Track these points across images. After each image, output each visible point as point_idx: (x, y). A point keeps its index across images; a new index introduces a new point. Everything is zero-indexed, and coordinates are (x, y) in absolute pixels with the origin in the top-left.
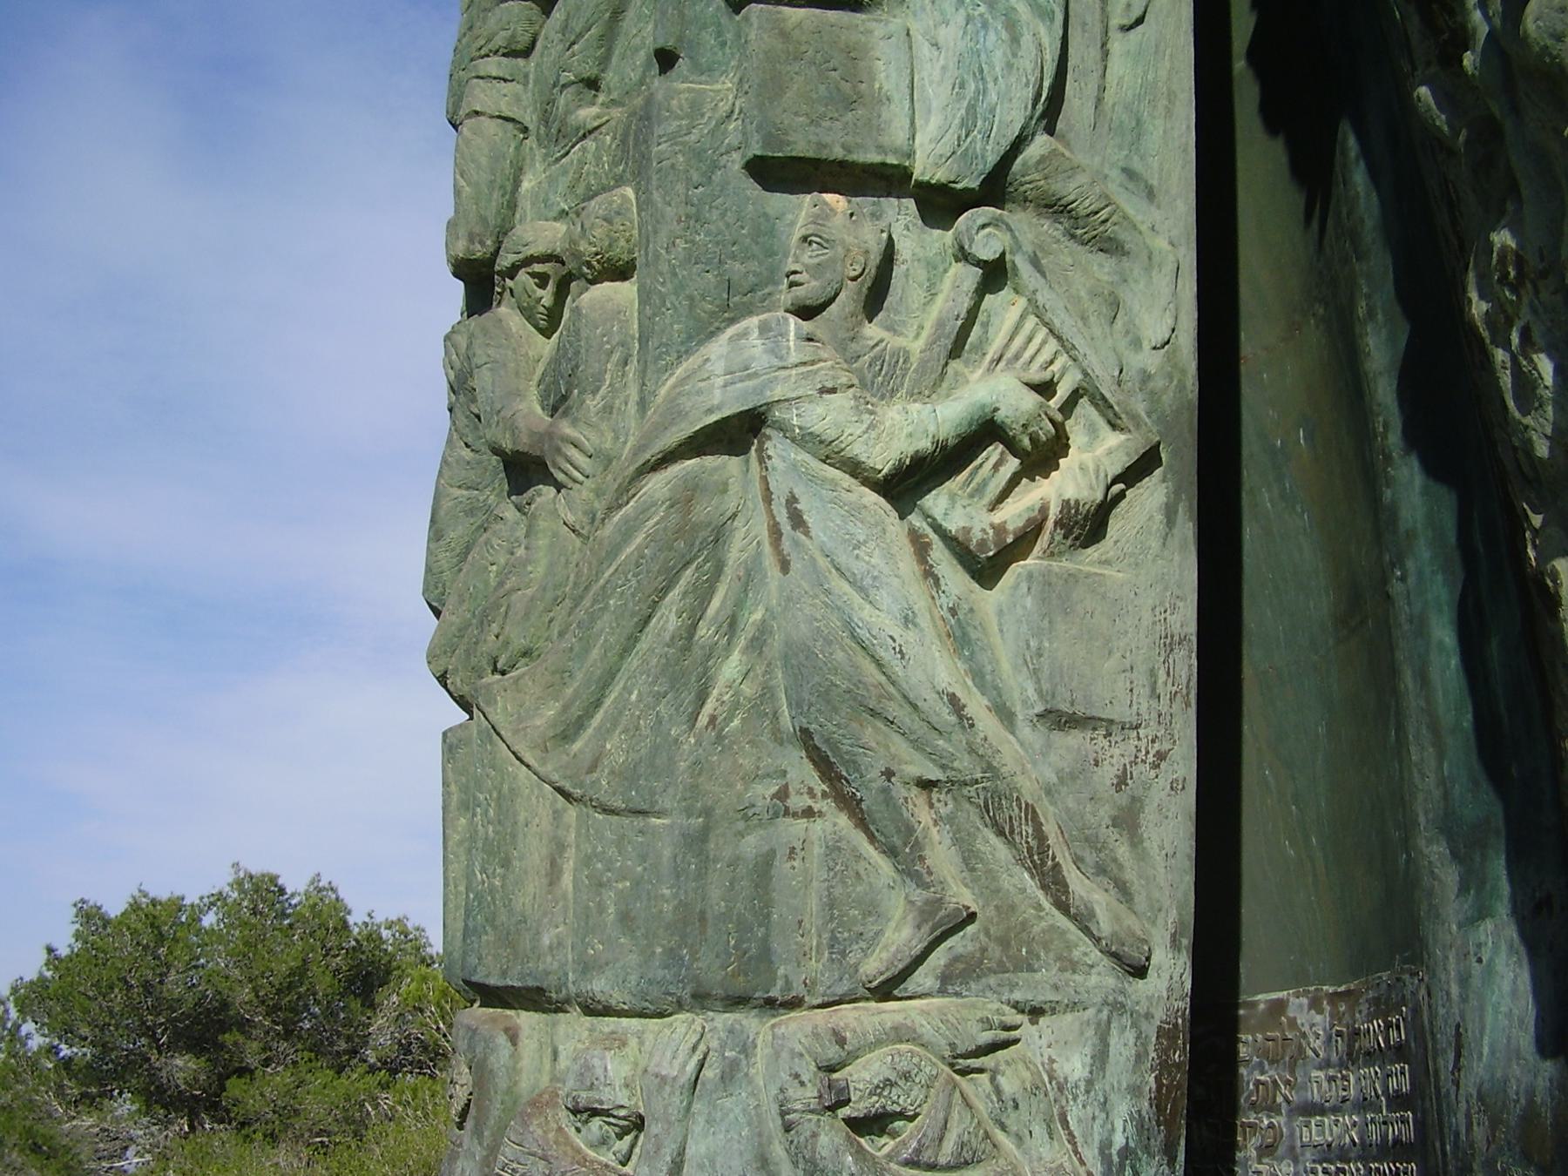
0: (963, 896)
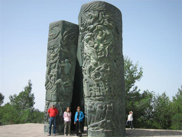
0: (65, 98)
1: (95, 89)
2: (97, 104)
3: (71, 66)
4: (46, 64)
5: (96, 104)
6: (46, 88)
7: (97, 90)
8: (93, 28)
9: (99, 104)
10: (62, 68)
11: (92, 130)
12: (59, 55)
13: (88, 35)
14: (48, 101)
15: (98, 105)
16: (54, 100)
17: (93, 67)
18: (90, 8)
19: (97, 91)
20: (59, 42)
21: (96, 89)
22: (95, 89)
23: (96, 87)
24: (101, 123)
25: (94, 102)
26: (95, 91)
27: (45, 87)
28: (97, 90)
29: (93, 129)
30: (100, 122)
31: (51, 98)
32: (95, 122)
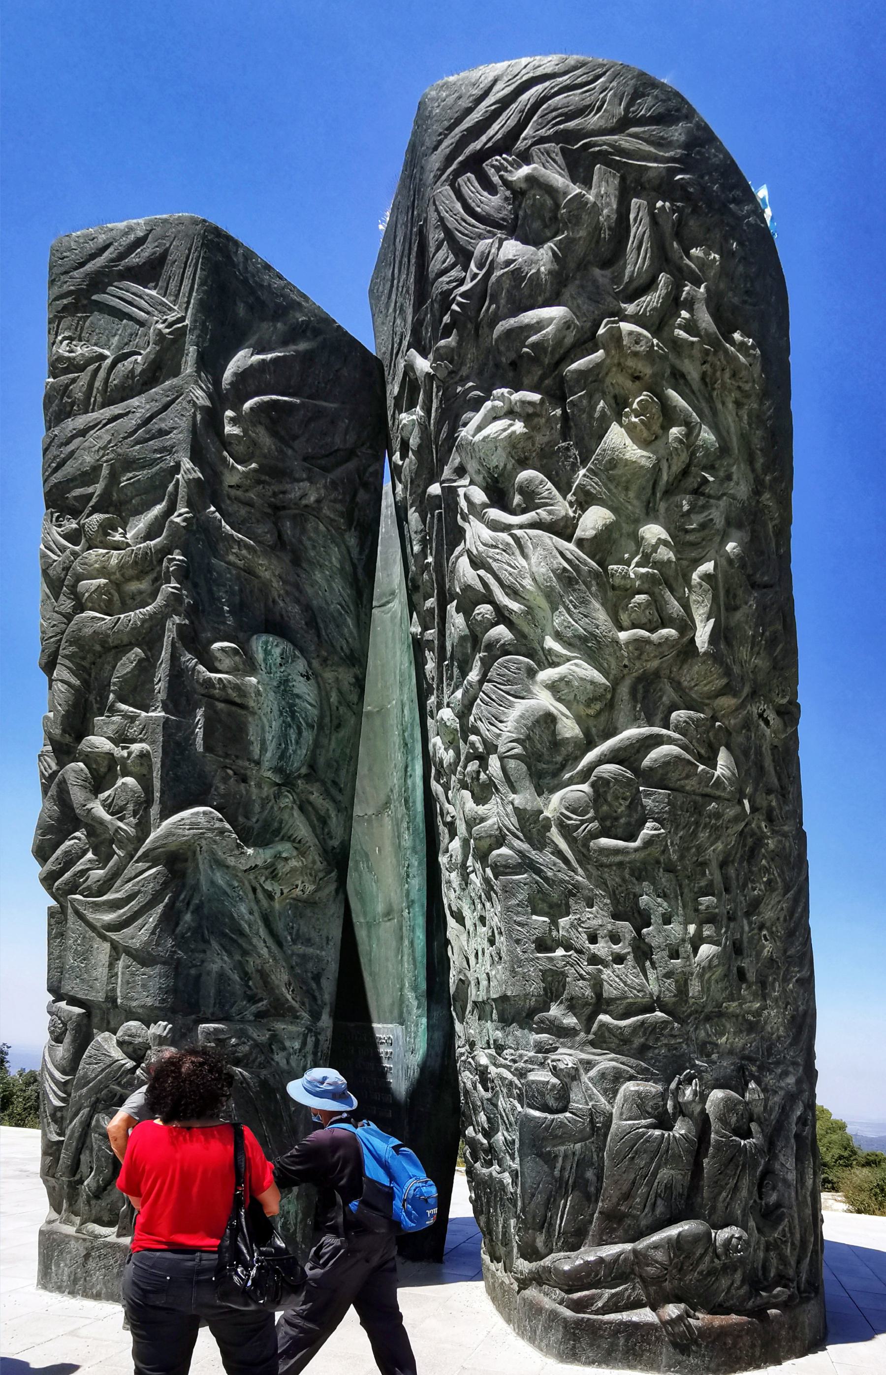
2: (617, 1078)
3: (316, 712)
4: (35, 653)
5: (603, 1075)
6: (48, 880)
8: (559, 340)
9: (631, 1078)
10: (220, 706)
11: (568, 1313)
12: (184, 574)
13: (511, 413)
14: (73, 1001)
15: (631, 1086)
16: (145, 999)
18: (521, 125)
19: (619, 959)
20: (180, 437)
21: (601, 932)
22: (593, 939)
25: (584, 1056)
26: (594, 960)
27: (36, 869)
28: (616, 948)
29: (579, 1306)
30: (656, 1247)
31: (113, 975)
32: (601, 1243)
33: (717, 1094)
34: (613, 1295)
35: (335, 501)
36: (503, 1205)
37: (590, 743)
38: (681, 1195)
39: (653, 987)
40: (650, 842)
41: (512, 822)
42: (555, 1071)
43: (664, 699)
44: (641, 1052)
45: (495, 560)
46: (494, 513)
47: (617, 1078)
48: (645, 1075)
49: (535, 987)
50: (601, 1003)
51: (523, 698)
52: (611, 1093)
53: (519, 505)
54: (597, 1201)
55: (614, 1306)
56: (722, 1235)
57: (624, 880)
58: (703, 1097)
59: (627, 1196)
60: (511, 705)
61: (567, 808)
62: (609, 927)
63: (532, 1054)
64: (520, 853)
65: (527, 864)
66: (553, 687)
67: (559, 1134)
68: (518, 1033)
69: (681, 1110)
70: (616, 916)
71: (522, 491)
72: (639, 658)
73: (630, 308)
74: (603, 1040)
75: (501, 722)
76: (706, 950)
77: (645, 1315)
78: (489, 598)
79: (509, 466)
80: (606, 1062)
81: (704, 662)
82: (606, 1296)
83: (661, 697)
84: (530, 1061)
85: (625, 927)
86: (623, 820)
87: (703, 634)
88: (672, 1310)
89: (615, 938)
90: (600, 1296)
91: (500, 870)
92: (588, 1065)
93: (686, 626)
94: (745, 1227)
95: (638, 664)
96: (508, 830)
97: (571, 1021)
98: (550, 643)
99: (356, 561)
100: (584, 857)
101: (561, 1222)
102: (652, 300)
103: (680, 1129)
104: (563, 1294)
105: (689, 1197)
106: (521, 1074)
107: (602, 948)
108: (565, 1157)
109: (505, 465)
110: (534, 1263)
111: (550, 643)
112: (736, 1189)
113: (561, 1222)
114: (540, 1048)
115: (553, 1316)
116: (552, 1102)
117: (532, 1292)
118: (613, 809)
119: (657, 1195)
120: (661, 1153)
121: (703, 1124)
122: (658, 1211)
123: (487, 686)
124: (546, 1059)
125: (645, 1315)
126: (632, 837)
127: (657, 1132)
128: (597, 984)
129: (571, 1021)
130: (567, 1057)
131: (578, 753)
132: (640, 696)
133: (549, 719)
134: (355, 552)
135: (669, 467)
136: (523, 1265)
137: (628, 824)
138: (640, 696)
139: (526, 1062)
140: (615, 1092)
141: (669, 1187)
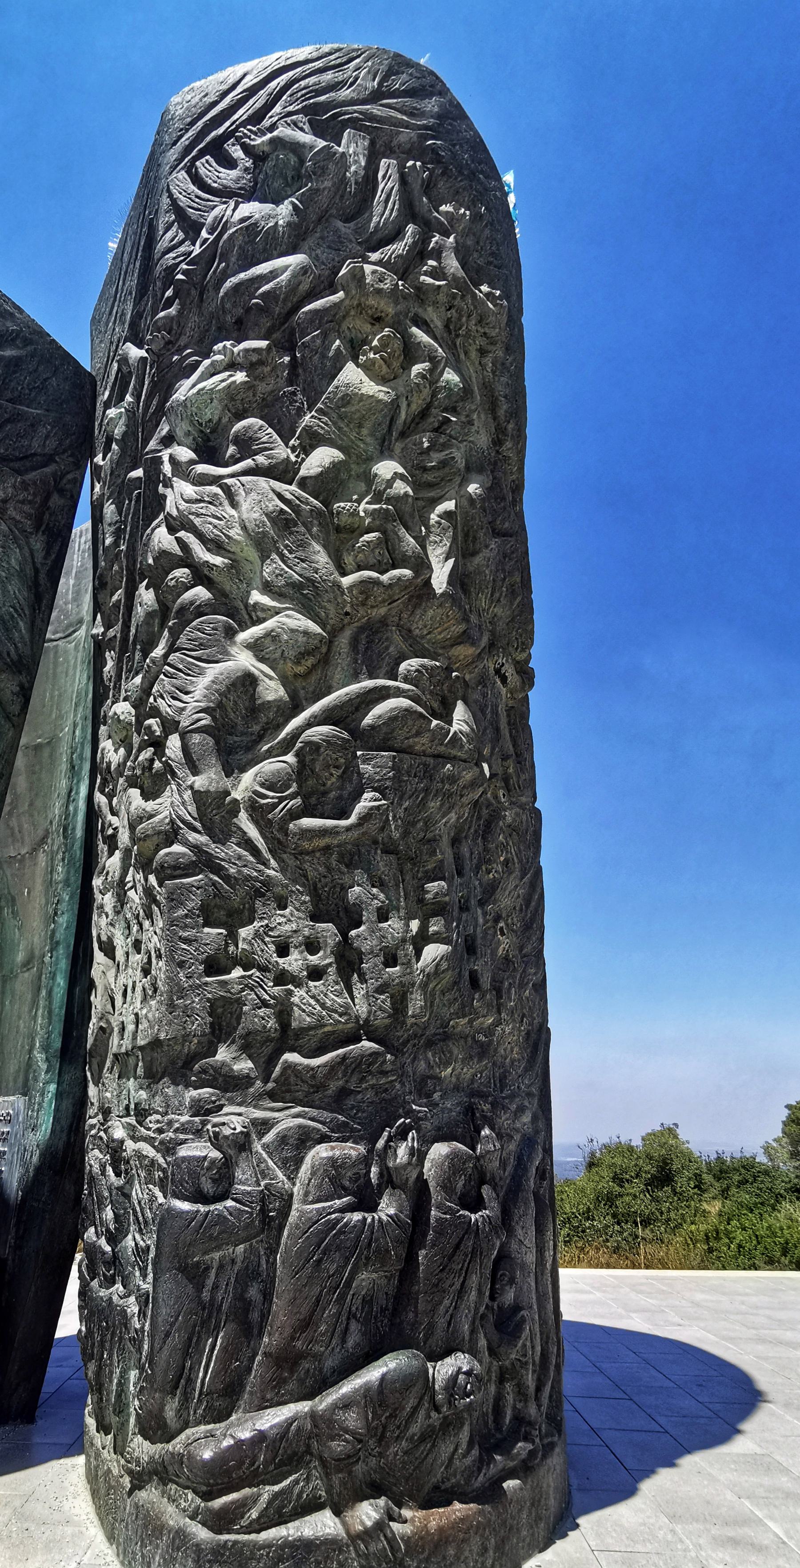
1: (283, 950)
2: (304, 1140)
5: (283, 1139)
7: (314, 959)
9: (323, 1139)
11: (202, 1534)
13: (232, 366)
15: (322, 1151)
17: (272, 690)
19: (316, 973)
21: (295, 940)
23: (289, 921)
24: (352, 1419)
25: (258, 1114)
26: (282, 977)
28: (314, 959)
29: (220, 1522)
30: (346, 1404)
32: (263, 1405)
33: (439, 1150)
34: (276, 1496)
35: (23, 502)
36: (122, 1350)
37: (296, 708)
38: (383, 1310)
39: (361, 1008)
40: (365, 818)
41: (189, 812)
42: (216, 1141)
43: (391, 649)
44: (337, 1103)
45: (198, 515)
46: (202, 468)
47: (304, 1140)
48: (344, 1133)
49: (198, 1024)
50: (287, 1036)
51: (217, 662)
52: (292, 1165)
53: (232, 456)
54: (260, 1335)
55: (278, 1515)
56: (444, 1370)
57: (329, 869)
58: (418, 1155)
59: (306, 1324)
60: (201, 673)
61: (262, 785)
62: (306, 932)
63: (185, 1118)
64: (196, 848)
65: (204, 861)
66: (255, 647)
67: (216, 1232)
68: (170, 1091)
69: (389, 1179)
70: (315, 917)
71: (237, 441)
72: (363, 604)
73: (374, 256)
74: (286, 1091)
75: (187, 693)
76: (433, 952)
77: (323, 1524)
78: (186, 559)
79: (225, 420)
80: (288, 1120)
81: (441, 605)
82: (265, 1497)
83: (387, 648)
84: (183, 1129)
85: (328, 930)
86: (332, 795)
87: (440, 579)
88: (367, 1513)
89: (312, 946)
90: (255, 1499)
91: (166, 873)
92: (263, 1126)
93: (422, 566)
94: (473, 1352)
95: (362, 612)
96: (183, 821)
97: (245, 1065)
98: (256, 597)
99: (39, 566)
100: (277, 847)
101: (205, 1375)
102: (399, 248)
103: (388, 1208)
104: (198, 1501)
105: (395, 1312)
106: (168, 1148)
107: (294, 962)
108: (221, 1267)
109: (220, 419)
110: (160, 1446)
111: (256, 597)
112: (462, 1292)
113: (205, 1375)
114: (201, 1109)
115: (181, 1537)
116: (207, 1186)
117: (149, 1495)
118: (320, 783)
119: (351, 1316)
120: (360, 1247)
121: (419, 1195)
122: (350, 1343)
123: (173, 658)
124: (204, 1123)
125: (323, 1524)
126: (344, 814)
127: (357, 1216)
128: (283, 1011)
129: (245, 1065)
130: (233, 1119)
131: (281, 720)
132: (362, 648)
133: (248, 681)
134: (39, 557)
135: (409, 405)
136: (142, 1448)
137: (340, 798)
138: (362, 648)
139: (176, 1131)
140: (299, 1162)
141: (368, 1301)
